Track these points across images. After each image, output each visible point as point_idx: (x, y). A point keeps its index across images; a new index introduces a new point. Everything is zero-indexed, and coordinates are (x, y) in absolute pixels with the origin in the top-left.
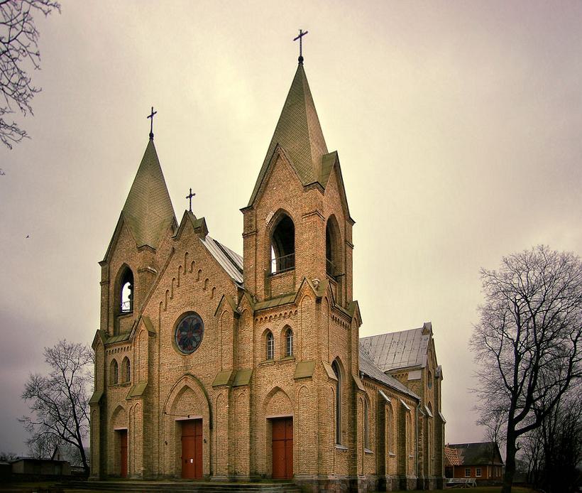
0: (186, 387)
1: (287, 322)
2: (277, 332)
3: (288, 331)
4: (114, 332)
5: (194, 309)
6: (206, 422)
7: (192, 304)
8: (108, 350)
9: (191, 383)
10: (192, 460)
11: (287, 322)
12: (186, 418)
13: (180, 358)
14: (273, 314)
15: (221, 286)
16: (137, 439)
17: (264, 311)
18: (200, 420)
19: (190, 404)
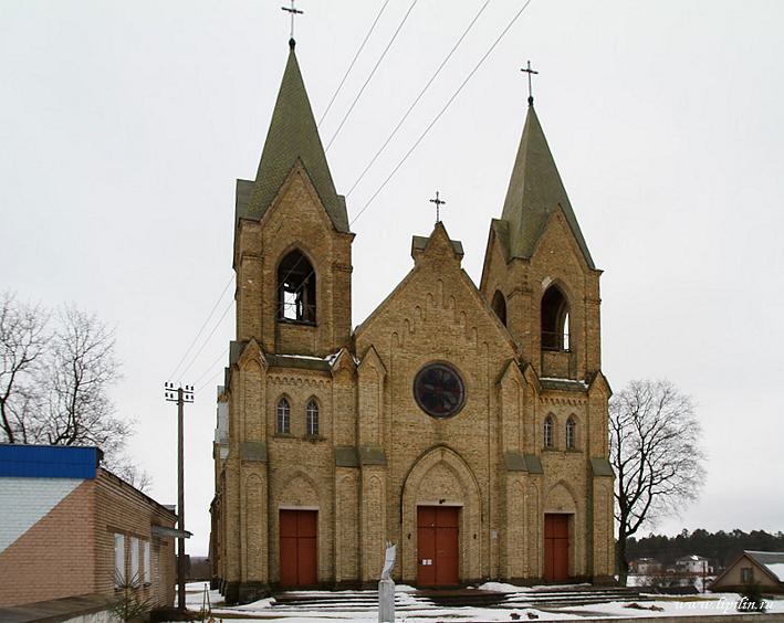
0: (442, 462)
1: (574, 410)
2: (563, 418)
3: (571, 421)
4: (275, 346)
5: (453, 360)
6: (471, 513)
7: (448, 353)
8: (274, 376)
9: (450, 457)
10: (430, 562)
11: (574, 410)
12: (437, 504)
13: (427, 419)
14: (560, 398)
15: (496, 344)
16: (373, 530)
17: (553, 387)
18: (458, 509)
19: (443, 486)
